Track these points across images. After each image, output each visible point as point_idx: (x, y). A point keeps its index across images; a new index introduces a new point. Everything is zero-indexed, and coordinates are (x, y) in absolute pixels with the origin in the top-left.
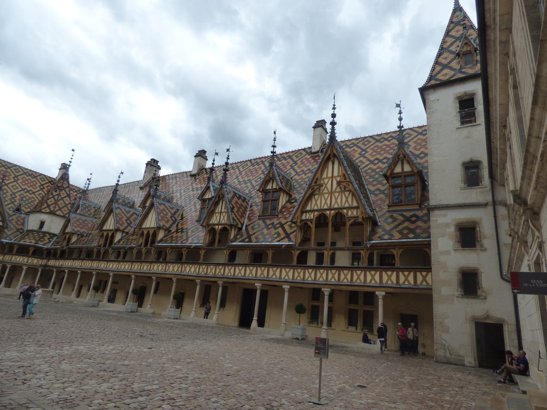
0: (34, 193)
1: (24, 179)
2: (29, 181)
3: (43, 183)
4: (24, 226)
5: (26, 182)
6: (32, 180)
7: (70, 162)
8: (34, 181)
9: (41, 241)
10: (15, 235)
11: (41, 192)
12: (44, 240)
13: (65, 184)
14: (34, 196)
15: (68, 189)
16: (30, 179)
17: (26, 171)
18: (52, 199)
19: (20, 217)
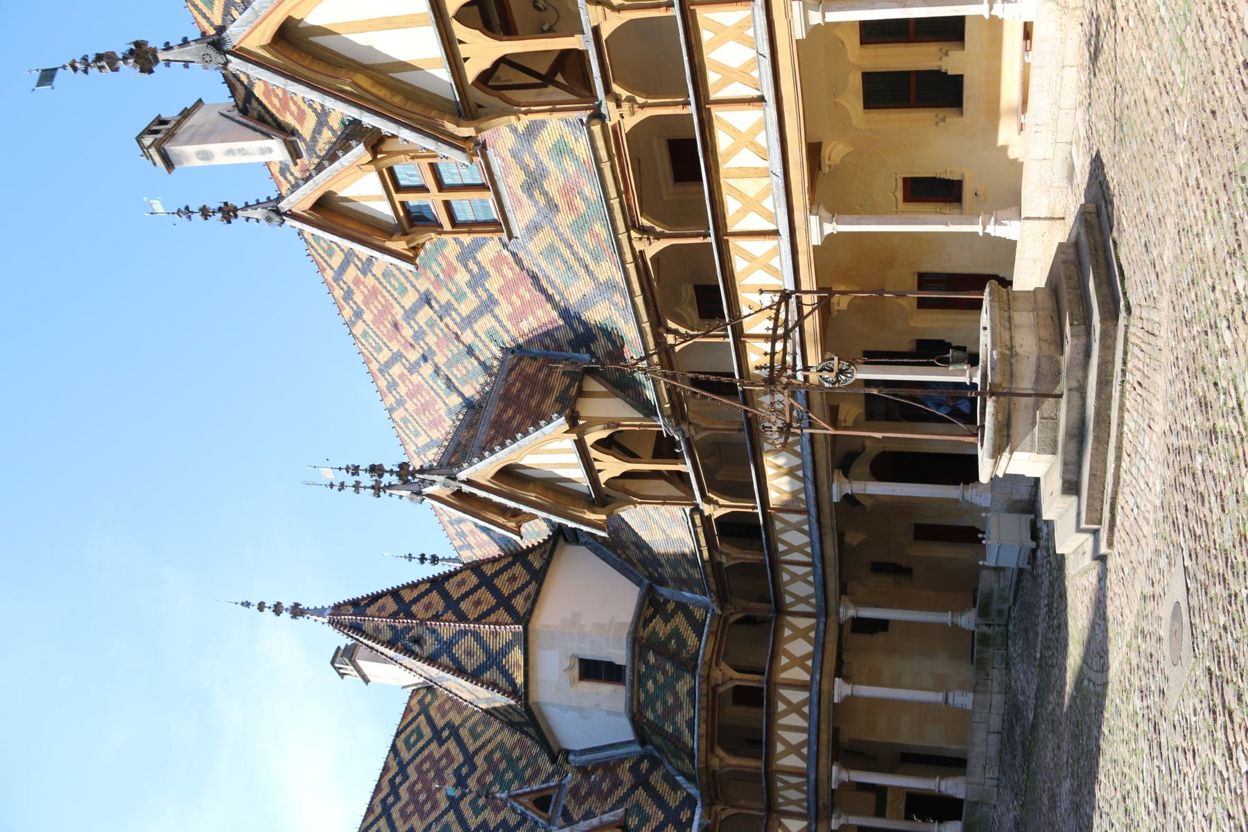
0: (469, 758)
1: (411, 808)
2: (419, 786)
3: (427, 732)
4: (621, 760)
5: (422, 797)
6: (413, 776)
7: (278, 609)
8: (419, 768)
9: (682, 643)
10: (663, 788)
11: (464, 733)
12: (676, 634)
13: (383, 608)
14: (483, 753)
15: (402, 593)
16: (411, 789)
17: (378, 810)
18: (458, 651)
19: (575, 792)
